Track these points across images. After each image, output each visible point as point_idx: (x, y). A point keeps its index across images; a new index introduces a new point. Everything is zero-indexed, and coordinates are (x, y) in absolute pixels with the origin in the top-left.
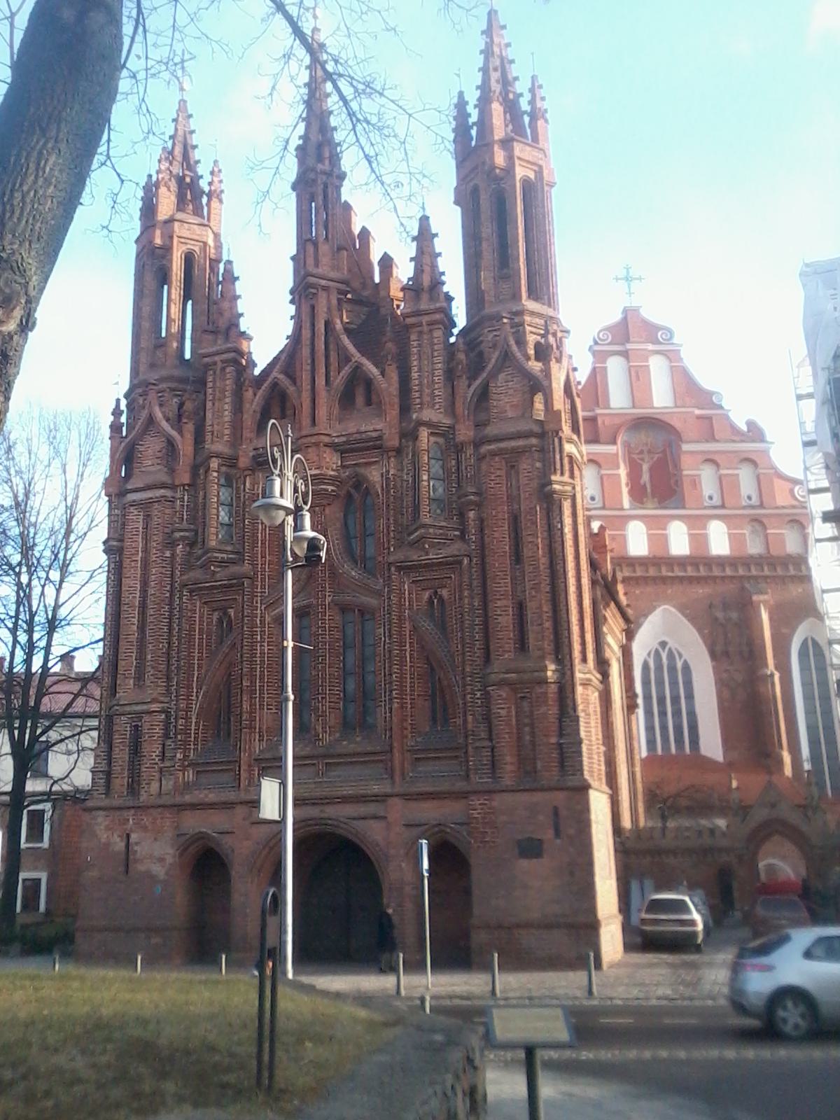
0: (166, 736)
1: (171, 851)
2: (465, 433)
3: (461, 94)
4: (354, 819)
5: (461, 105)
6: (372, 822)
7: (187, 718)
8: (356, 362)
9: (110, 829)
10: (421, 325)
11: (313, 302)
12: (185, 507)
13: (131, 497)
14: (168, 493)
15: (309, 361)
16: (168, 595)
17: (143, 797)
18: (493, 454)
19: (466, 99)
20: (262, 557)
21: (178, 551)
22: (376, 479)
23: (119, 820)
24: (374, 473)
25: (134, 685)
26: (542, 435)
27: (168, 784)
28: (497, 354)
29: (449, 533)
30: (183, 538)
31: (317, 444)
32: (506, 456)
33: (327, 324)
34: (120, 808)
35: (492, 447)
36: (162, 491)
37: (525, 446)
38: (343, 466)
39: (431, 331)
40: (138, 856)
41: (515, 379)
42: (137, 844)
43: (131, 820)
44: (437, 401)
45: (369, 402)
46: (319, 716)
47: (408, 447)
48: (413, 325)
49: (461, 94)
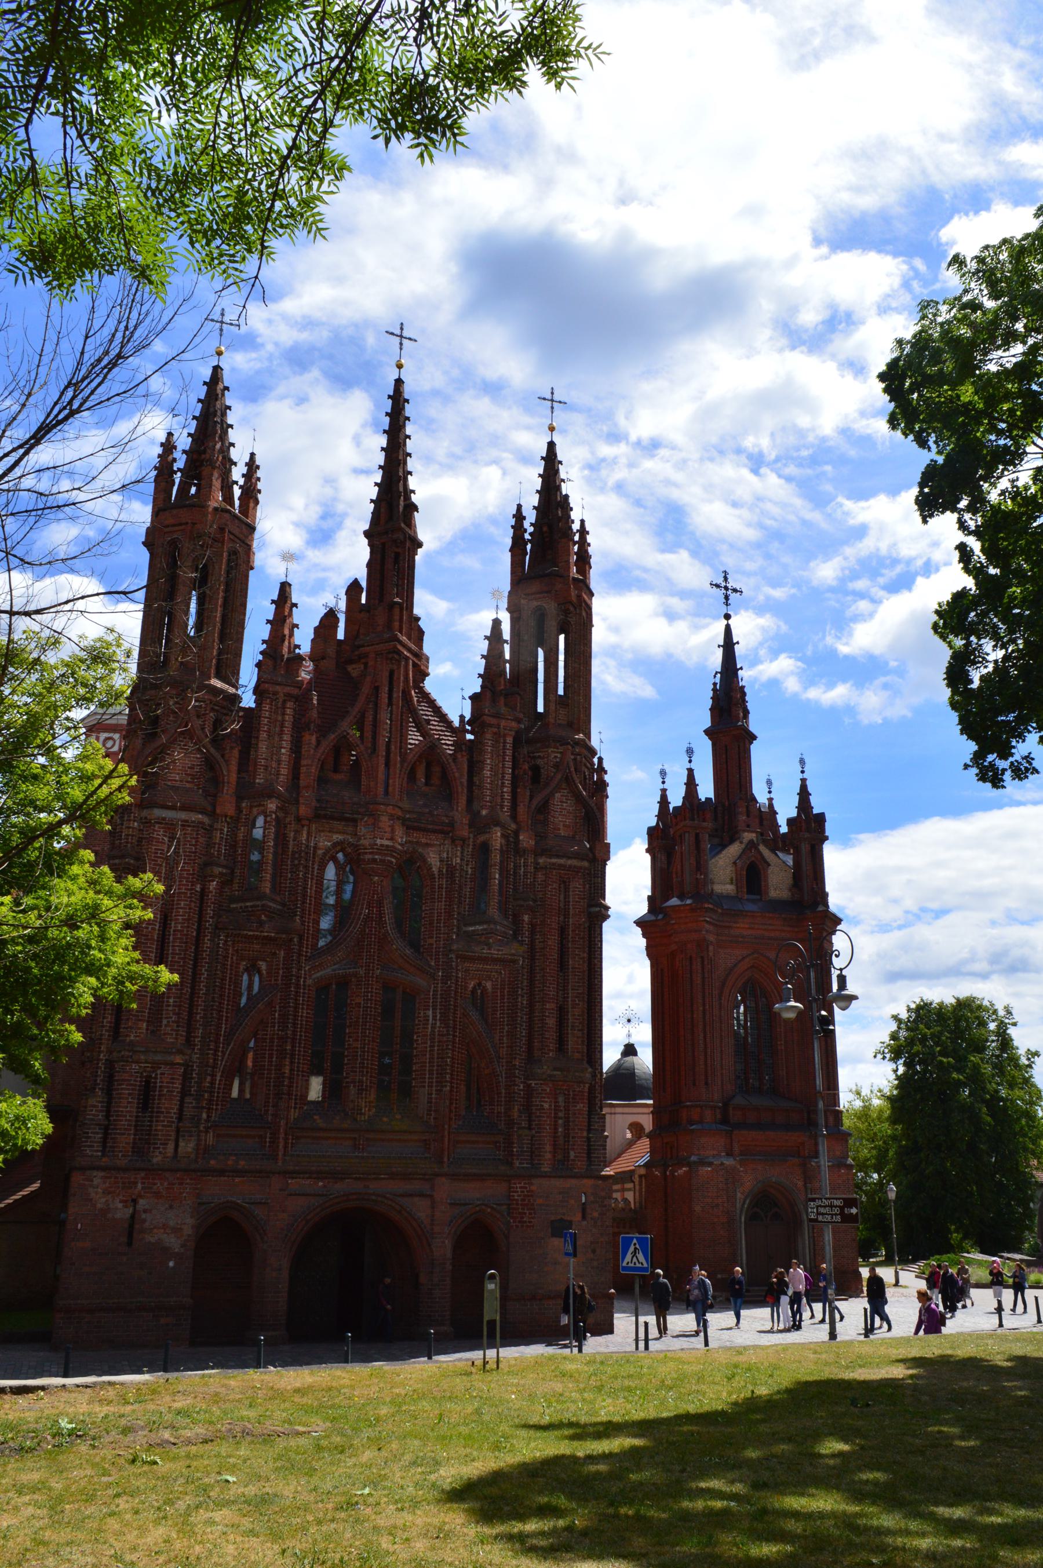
0: (184, 1093)
1: (190, 1221)
2: (526, 840)
4: (402, 1196)
5: (519, 517)
6: (416, 1199)
7: (213, 1076)
9: (109, 1193)
10: (498, 726)
11: (395, 667)
13: (158, 813)
14: (206, 820)
16: (194, 934)
17: (157, 1159)
23: (124, 1183)
25: (147, 1029)
27: (187, 1147)
28: (559, 776)
34: (125, 1170)
37: (581, 868)
40: (147, 1224)
42: (145, 1211)
43: (140, 1186)
46: (362, 1090)
48: (491, 726)
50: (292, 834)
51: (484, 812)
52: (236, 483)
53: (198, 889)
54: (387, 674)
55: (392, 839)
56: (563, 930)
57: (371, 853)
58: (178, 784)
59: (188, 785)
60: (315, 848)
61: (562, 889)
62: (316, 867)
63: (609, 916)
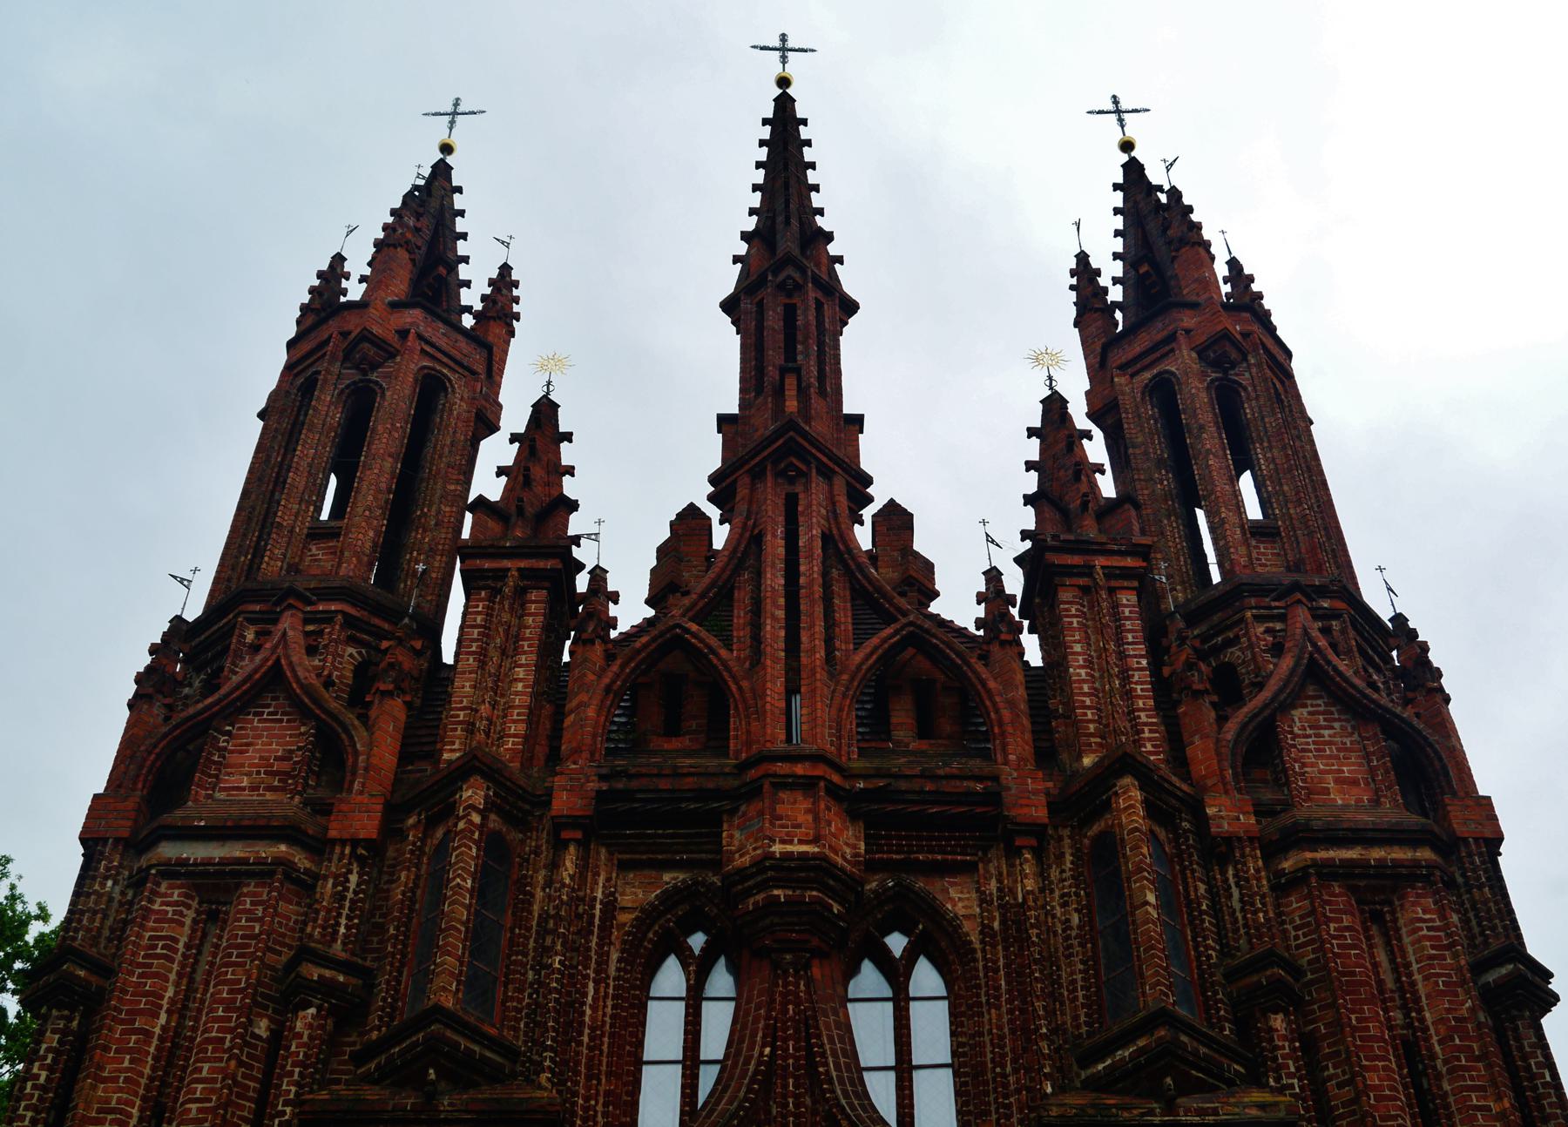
3: (1082, 258)
5: (1084, 271)
8: (911, 624)
10: (1088, 571)
11: (799, 488)
12: (347, 904)
14: (301, 860)
15: (782, 601)
18: (1328, 872)
19: (1094, 265)
20: (589, 1078)
21: (299, 1025)
22: (960, 909)
24: (953, 893)
26: (1449, 846)
28: (1287, 663)
29: (1226, 1062)
30: (326, 987)
31: (807, 785)
32: (1362, 884)
33: (827, 538)
35: (1322, 854)
36: (283, 848)
37: (1416, 864)
38: (871, 866)
39: (1112, 591)
41: (1336, 725)
44: (1147, 735)
45: (925, 730)
47: (1060, 839)
48: (1069, 571)
49: (1082, 258)
50: (541, 877)
51: (1087, 761)
52: (469, 309)
53: (263, 1033)
54: (781, 502)
55: (815, 841)
56: (1411, 1050)
57: (764, 886)
58: (246, 794)
59: (269, 796)
60: (610, 907)
61: (1377, 940)
62: (615, 956)
63: (1554, 999)
